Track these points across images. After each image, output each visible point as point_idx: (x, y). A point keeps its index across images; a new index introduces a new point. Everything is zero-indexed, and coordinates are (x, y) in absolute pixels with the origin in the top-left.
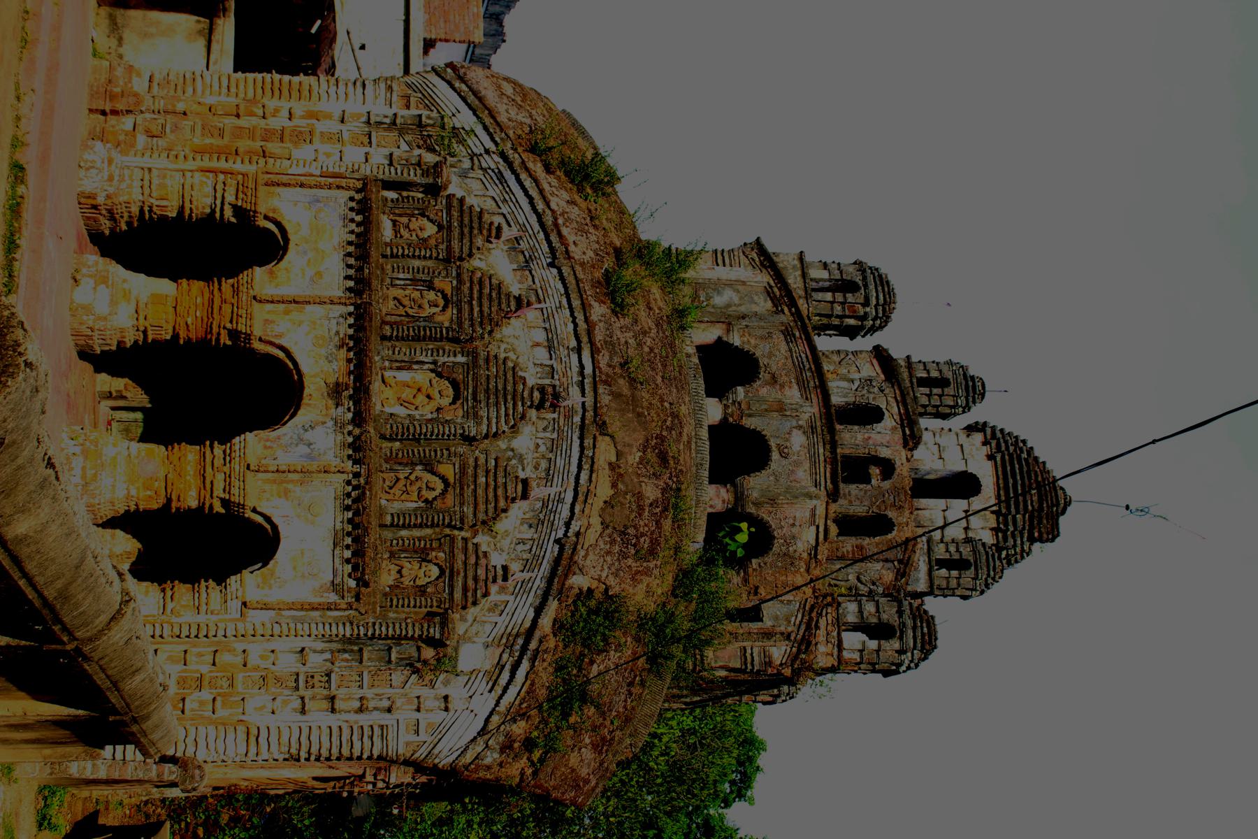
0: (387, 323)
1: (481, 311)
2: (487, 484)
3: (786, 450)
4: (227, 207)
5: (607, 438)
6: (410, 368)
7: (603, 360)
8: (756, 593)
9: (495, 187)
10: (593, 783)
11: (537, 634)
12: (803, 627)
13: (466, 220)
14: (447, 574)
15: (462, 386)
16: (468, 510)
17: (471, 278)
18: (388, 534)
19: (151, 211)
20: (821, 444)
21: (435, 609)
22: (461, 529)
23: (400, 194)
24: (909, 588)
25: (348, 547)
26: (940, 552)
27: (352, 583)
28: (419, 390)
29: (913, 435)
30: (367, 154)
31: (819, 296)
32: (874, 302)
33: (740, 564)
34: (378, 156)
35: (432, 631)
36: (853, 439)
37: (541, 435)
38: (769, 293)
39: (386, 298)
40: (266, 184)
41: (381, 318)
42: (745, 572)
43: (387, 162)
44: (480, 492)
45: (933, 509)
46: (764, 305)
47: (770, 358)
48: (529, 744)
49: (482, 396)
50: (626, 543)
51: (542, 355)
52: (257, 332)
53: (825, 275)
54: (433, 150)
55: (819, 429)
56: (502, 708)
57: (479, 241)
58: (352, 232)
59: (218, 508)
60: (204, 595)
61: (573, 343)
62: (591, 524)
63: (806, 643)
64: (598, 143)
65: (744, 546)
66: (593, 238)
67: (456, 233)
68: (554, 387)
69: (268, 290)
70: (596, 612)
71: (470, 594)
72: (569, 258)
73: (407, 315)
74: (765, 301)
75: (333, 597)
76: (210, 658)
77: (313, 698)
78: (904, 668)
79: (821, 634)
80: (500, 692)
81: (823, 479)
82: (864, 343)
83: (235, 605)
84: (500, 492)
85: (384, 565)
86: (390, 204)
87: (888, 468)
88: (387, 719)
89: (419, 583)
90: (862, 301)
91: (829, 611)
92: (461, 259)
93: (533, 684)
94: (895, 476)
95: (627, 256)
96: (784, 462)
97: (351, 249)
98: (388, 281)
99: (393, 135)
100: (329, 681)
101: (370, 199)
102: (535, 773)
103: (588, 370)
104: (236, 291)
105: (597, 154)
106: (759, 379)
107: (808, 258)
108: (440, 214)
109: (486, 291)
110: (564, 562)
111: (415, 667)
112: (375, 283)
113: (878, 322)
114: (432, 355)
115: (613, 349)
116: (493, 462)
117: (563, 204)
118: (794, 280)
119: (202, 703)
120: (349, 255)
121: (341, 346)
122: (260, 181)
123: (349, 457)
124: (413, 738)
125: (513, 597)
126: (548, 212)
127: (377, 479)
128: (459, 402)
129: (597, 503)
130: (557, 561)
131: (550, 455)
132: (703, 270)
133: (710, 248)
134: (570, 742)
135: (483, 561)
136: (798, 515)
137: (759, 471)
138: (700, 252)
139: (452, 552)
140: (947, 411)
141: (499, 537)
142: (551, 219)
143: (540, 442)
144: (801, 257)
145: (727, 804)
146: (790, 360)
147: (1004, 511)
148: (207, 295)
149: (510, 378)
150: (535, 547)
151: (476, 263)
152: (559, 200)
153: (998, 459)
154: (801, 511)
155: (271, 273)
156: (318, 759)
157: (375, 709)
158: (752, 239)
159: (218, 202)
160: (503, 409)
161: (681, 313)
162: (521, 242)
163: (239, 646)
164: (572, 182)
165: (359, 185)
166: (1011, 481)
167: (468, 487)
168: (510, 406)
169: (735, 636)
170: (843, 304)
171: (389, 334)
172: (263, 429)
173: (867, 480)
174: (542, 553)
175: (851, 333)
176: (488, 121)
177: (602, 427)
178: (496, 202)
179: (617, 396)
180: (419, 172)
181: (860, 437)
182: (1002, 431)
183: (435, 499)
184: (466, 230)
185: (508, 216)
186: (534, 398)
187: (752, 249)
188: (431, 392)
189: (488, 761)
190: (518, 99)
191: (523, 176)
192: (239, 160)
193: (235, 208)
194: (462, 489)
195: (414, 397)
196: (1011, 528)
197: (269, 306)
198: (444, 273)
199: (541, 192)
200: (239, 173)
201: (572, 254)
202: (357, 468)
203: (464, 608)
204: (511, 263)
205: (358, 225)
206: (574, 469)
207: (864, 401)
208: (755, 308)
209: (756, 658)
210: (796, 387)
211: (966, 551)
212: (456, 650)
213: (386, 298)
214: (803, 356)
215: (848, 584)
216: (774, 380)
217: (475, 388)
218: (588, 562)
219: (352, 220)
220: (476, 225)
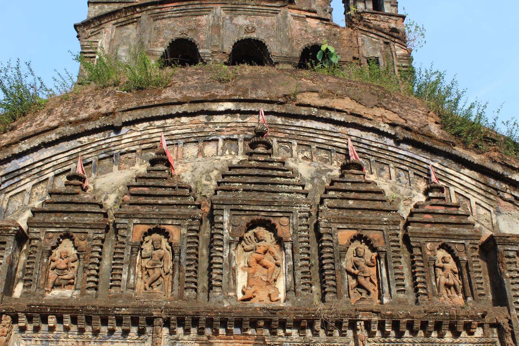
1: (169, 196)
3: (250, 28)
7: (221, 93)
8: (358, 59)
9: (23, 182)
11: (489, 165)
14: (446, 241)
15: (255, 218)
17: (131, 204)
20: (245, 6)
23: (19, 280)
25: (441, 336)
27: (479, 332)
28: (258, 262)
35: (511, 254)
37: (295, 153)
38: (121, 25)
41: (175, 299)
42: (344, 64)
44: (364, 205)
46: (131, 30)
47: (176, 31)
49: (268, 197)
51: (210, 149)
55: (233, 6)
57: (87, 197)
61: (202, 118)
67: (74, 218)
68: (245, 139)
71: (464, 221)
72: (113, 113)
74: (127, 29)
79: (383, 25)
81: (271, 8)
84: (363, 188)
85: (448, 302)
86: (33, 289)
91: (367, 18)
96: (259, 31)
98: (130, 292)
101: (29, 306)
103: (230, 106)
106: (192, 39)
108: (51, 235)
109: (146, 190)
110: (420, 139)
114: (222, 246)
115: (208, 86)
116: (331, 193)
117: (51, 118)
120: (96, 333)
123: (343, 334)
125: (452, 189)
128: (273, 221)
131: (314, 147)
135: (428, 208)
136: (298, 28)
137: (266, 47)
139: (425, 235)
141: (398, 196)
142: (68, 127)
143: (301, 156)
146: (178, 19)
149: (244, 171)
150: (402, 167)
151: (110, 202)
160: (278, 179)
162: (89, 160)
167: (364, 216)
168: (275, 173)
171: (194, 292)
174: (408, 160)
177: (288, 98)
178: (40, 182)
179: (255, 87)
183: (373, 249)
184: (73, 208)
185: (57, 172)
186: (261, 151)
187: (84, 32)
188: (261, 250)
191: (16, 150)
194: (364, 222)
195: (265, 267)
199: (36, 134)
201: (110, 110)
204: (112, 171)
205: (60, 320)
206: (328, 127)
208: (134, 35)
210: (199, 17)
214: (175, 9)
218: (416, 120)
219: (52, 329)
220: (68, 199)
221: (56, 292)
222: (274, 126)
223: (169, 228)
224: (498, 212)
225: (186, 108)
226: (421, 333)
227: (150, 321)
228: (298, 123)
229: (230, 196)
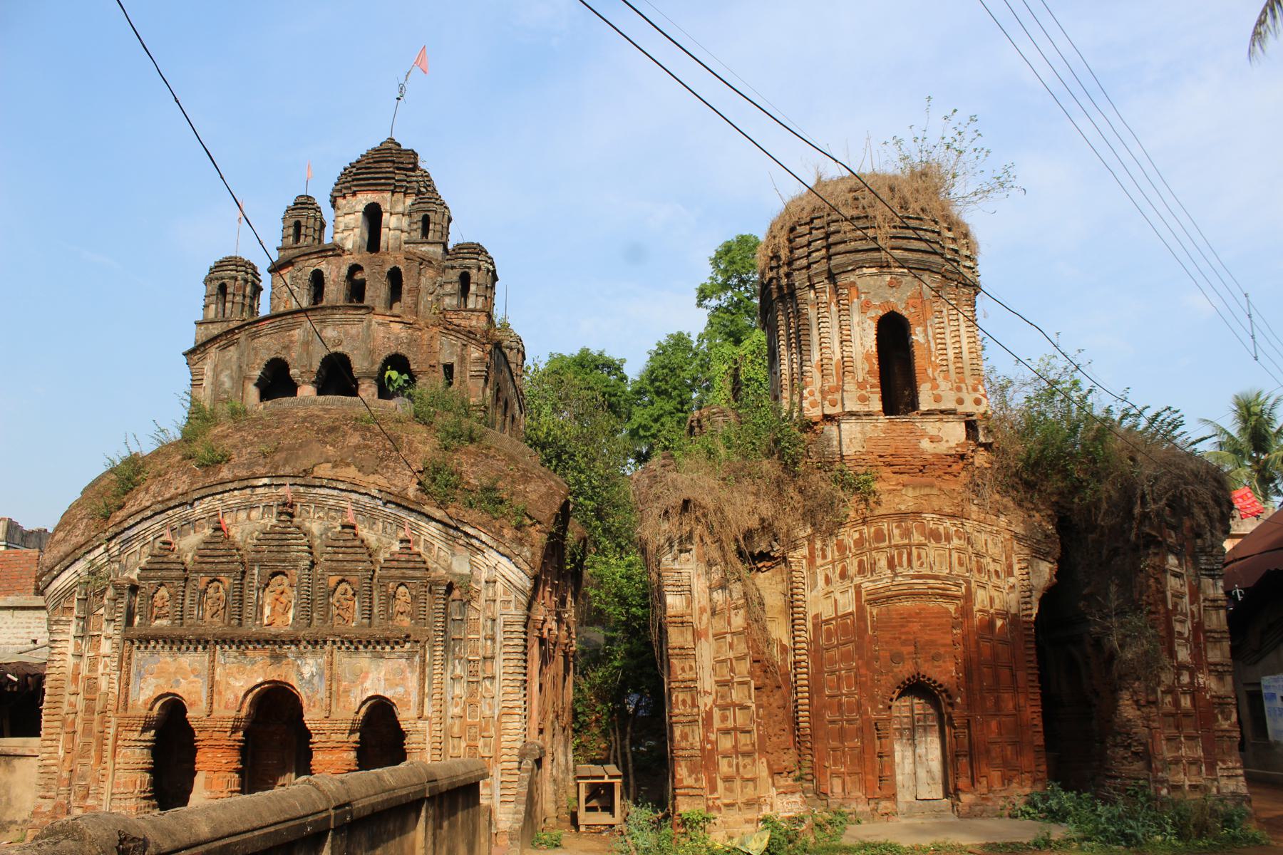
0: (229, 623)
1: (223, 556)
2: (343, 553)
4: (142, 738)
5: (315, 469)
6: (262, 607)
10: (553, 483)
11: (447, 520)
12: (459, 335)
13: (157, 566)
16: (361, 566)
18: (376, 621)
19: (144, 792)
21: (427, 589)
22: (374, 571)
24: (440, 259)
25: (383, 649)
26: (417, 235)
27: (408, 645)
29: (333, 250)
30: (106, 638)
31: (228, 312)
32: (234, 273)
33: (413, 379)
34: (109, 630)
36: (335, 291)
37: (312, 514)
38: (225, 348)
39: (211, 623)
40: (126, 709)
43: (113, 624)
44: (348, 558)
45: (388, 236)
46: (232, 352)
48: (519, 527)
49: (282, 556)
50: (388, 458)
51: (254, 514)
52: (233, 713)
53: (213, 307)
54: (105, 589)
56: (494, 545)
57: (173, 557)
58: (163, 647)
59: (356, 737)
60: (414, 746)
61: (248, 491)
62: (374, 482)
63: (470, 334)
64: (104, 470)
65: (401, 373)
66: (173, 475)
67: (165, 573)
68: (279, 505)
69: (204, 705)
70: (434, 480)
71: (418, 566)
73: (225, 608)
75: (417, 659)
76: (456, 741)
77: (484, 671)
78: (491, 267)
79: (463, 323)
80: (484, 546)
82: (266, 280)
83: (420, 724)
84: (349, 544)
86: (144, 621)
87: (355, 269)
88: (500, 621)
89: (409, 601)
90: (233, 281)
92: (185, 570)
93: (479, 524)
94: (361, 264)
95: (188, 451)
96: (345, 343)
97: (175, 648)
98: (199, 622)
99: (92, 619)
100: (474, 661)
102: (540, 523)
103: (266, 481)
104: (203, 729)
105: (111, 471)
107: (200, 318)
109: (208, 552)
111: (466, 603)
112: (200, 631)
113: (250, 271)
118: (215, 330)
119: (485, 745)
120: (179, 649)
121: (245, 654)
122: (123, 715)
123: (322, 648)
124: (512, 604)
125: (422, 537)
126: (152, 508)
127: (337, 629)
128: (287, 572)
129: (359, 477)
130: (398, 505)
132: (205, 395)
133: (189, 389)
134: (521, 499)
135: (396, 557)
138: (192, 397)
139: (389, 578)
140: (318, 223)
144: (198, 323)
145: (624, 378)
147: (392, 188)
148: (206, 750)
151: (189, 559)
152: (144, 499)
153: (355, 189)
154: (380, 332)
155: (191, 705)
156: (525, 668)
157: (492, 629)
158: (184, 359)
159: (139, 744)
161: (235, 413)
163: (449, 721)
164: (132, 489)
165: (128, 643)
166: (371, 181)
169: (462, 382)
170: (234, 295)
172: (302, 708)
173: (363, 282)
175: (257, 290)
176: (83, 550)
179: (286, 462)
180: (120, 600)
181: (332, 287)
182: (336, 185)
184: (164, 566)
188: (278, 592)
189: (528, 554)
190: (68, 528)
191: (126, 525)
192: (107, 730)
193: (145, 730)
194: (346, 571)
196: (404, 184)
197: (215, 706)
198: (195, 582)
199: (137, 512)
200: (117, 729)
202: (329, 643)
203: (427, 570)
205: (158, 643)
206: (335, 493)
207: (308, 283)
208: (234, 358)
209: (478, 368)
211: (418, 217)
212: (455, 575)
213: (211, 623)
215: (435, 301)
216: (287, 348)
217: (276, 560)
219: (154, 647)
220: (160, 559)
221: (158, 622)
222: (298, 494)
223: (222, 579)
224: (453, 555)
225: (235, 485)
226: (370, 647)
227: (207, 642)
228: (315, 491)
229: (259, 556)
